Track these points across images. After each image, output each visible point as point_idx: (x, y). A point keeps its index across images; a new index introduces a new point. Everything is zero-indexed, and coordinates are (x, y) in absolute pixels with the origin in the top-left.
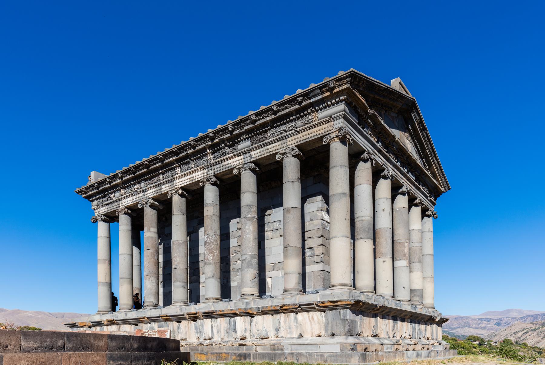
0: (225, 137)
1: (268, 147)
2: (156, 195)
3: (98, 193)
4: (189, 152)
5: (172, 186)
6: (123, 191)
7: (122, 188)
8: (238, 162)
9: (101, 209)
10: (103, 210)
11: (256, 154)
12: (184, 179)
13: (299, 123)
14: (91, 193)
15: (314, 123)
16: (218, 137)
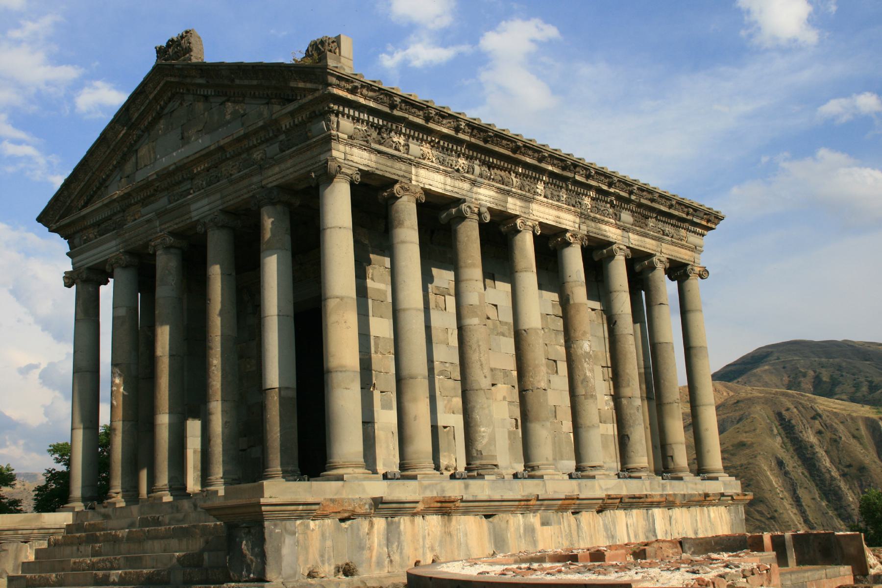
0: (623, 194)
4: (578, 178)
5: (527, 211)
6: (426, 149)
8: (615, 237)
9: (355, 150)
12: (547, 210)
14: (362, 101)
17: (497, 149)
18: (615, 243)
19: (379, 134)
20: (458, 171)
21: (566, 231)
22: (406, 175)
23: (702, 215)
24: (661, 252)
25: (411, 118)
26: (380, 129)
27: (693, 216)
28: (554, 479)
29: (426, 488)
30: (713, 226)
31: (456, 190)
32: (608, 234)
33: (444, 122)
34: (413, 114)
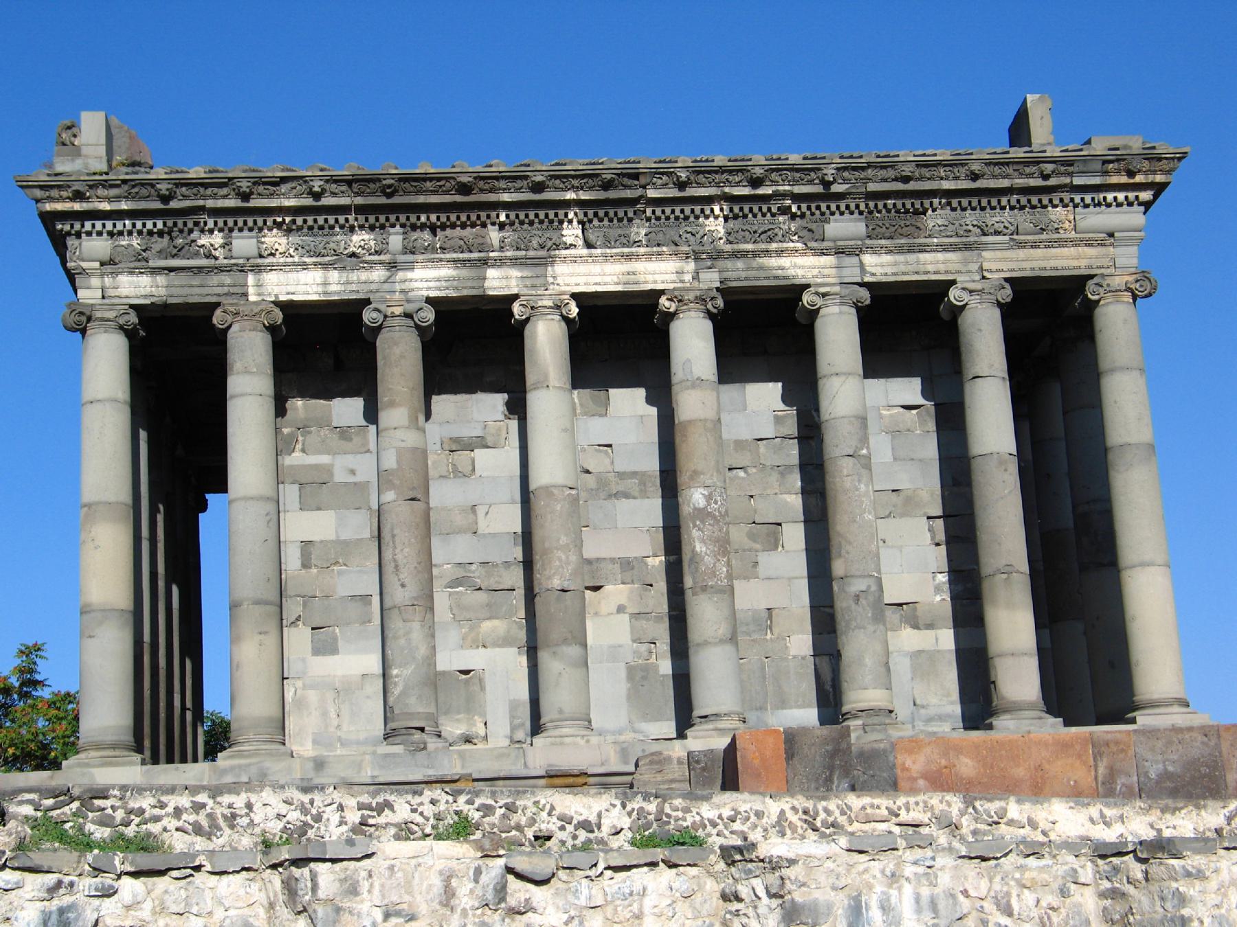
0: (798, 189)
1: (922, 256)
2: (452, 293)
3: (133, 214)
4: (652, 193)
5: (538, 282)
6: (275, 240)
7: (279, 226)
8: (815, 272)
9: (124, 279)
10: (138, 287)
11: (881, 266)
12: (596, 268)
13: (1023, 219)
14: (105, 206)
15: (1062, 235)
16: (774, 183)
17: (421, 199)
18: (808, 286)
19: (172, 239)
20: (353, 255)
21: (662, 292)
22: (232, 290)
23: (1098, 166)
24: (981, 268)
25: (210, 203)
26: (169, 233)
27: (1071, 174)
28: (562, 744)
29: (224, 772)
30: (1159, 178)
31: (354, 287)
32: (791, 272)
33: (284, 188)
34: (214, 196)
